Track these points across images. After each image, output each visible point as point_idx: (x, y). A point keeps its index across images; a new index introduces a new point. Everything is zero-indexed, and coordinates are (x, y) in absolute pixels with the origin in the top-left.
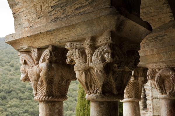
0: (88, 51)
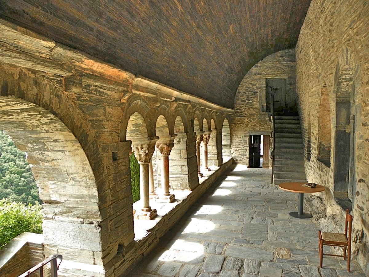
0: (140, 149)
